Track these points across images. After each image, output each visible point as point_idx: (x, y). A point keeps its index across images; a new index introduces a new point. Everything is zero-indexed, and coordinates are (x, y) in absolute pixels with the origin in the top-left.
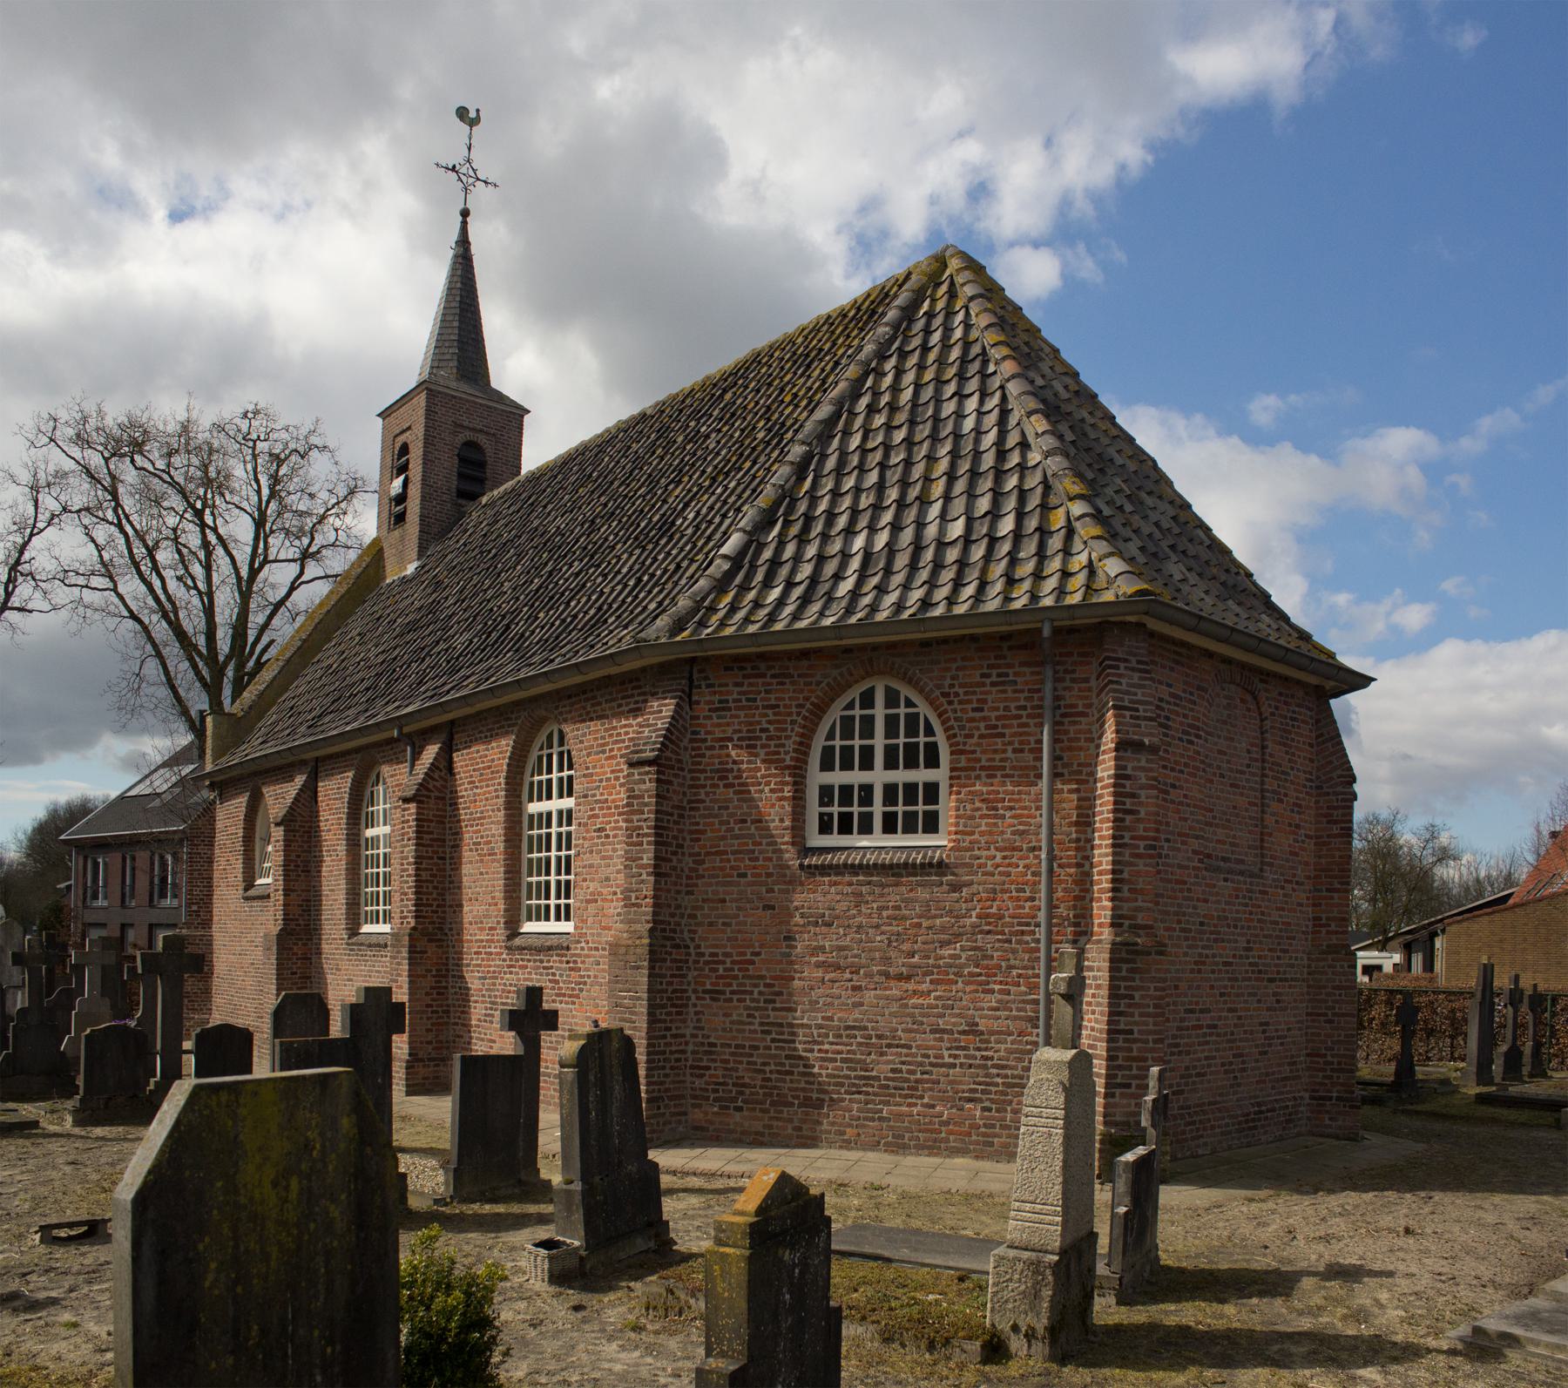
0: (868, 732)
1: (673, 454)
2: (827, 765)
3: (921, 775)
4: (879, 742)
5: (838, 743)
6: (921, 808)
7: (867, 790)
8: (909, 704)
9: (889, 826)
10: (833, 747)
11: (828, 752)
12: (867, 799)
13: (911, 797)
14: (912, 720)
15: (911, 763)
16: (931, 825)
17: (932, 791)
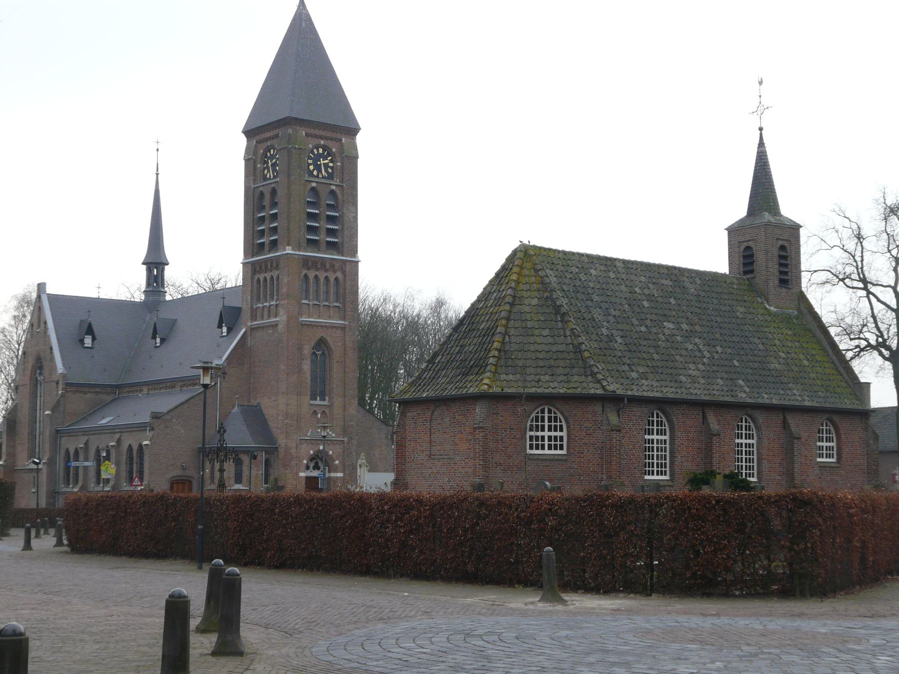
0: (543, 421)
1: (469, 317)
2: (531, 430)
3: (558, 434)
4: (546, 424)
5: (534, 423)
6: (558, 443)
7: (543, 437)
8: (555, 413)
9: (550, 448)
10: (533, 425)
11: (531, 426)
12: (543, 439)
13: (556, 440)
14: (556, 418)
15: (556, 430)
16: (561, 448)
17: (561, 438)
